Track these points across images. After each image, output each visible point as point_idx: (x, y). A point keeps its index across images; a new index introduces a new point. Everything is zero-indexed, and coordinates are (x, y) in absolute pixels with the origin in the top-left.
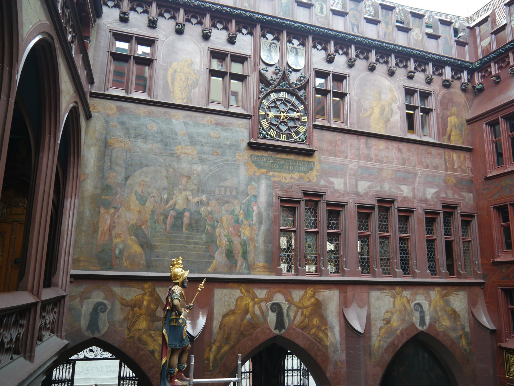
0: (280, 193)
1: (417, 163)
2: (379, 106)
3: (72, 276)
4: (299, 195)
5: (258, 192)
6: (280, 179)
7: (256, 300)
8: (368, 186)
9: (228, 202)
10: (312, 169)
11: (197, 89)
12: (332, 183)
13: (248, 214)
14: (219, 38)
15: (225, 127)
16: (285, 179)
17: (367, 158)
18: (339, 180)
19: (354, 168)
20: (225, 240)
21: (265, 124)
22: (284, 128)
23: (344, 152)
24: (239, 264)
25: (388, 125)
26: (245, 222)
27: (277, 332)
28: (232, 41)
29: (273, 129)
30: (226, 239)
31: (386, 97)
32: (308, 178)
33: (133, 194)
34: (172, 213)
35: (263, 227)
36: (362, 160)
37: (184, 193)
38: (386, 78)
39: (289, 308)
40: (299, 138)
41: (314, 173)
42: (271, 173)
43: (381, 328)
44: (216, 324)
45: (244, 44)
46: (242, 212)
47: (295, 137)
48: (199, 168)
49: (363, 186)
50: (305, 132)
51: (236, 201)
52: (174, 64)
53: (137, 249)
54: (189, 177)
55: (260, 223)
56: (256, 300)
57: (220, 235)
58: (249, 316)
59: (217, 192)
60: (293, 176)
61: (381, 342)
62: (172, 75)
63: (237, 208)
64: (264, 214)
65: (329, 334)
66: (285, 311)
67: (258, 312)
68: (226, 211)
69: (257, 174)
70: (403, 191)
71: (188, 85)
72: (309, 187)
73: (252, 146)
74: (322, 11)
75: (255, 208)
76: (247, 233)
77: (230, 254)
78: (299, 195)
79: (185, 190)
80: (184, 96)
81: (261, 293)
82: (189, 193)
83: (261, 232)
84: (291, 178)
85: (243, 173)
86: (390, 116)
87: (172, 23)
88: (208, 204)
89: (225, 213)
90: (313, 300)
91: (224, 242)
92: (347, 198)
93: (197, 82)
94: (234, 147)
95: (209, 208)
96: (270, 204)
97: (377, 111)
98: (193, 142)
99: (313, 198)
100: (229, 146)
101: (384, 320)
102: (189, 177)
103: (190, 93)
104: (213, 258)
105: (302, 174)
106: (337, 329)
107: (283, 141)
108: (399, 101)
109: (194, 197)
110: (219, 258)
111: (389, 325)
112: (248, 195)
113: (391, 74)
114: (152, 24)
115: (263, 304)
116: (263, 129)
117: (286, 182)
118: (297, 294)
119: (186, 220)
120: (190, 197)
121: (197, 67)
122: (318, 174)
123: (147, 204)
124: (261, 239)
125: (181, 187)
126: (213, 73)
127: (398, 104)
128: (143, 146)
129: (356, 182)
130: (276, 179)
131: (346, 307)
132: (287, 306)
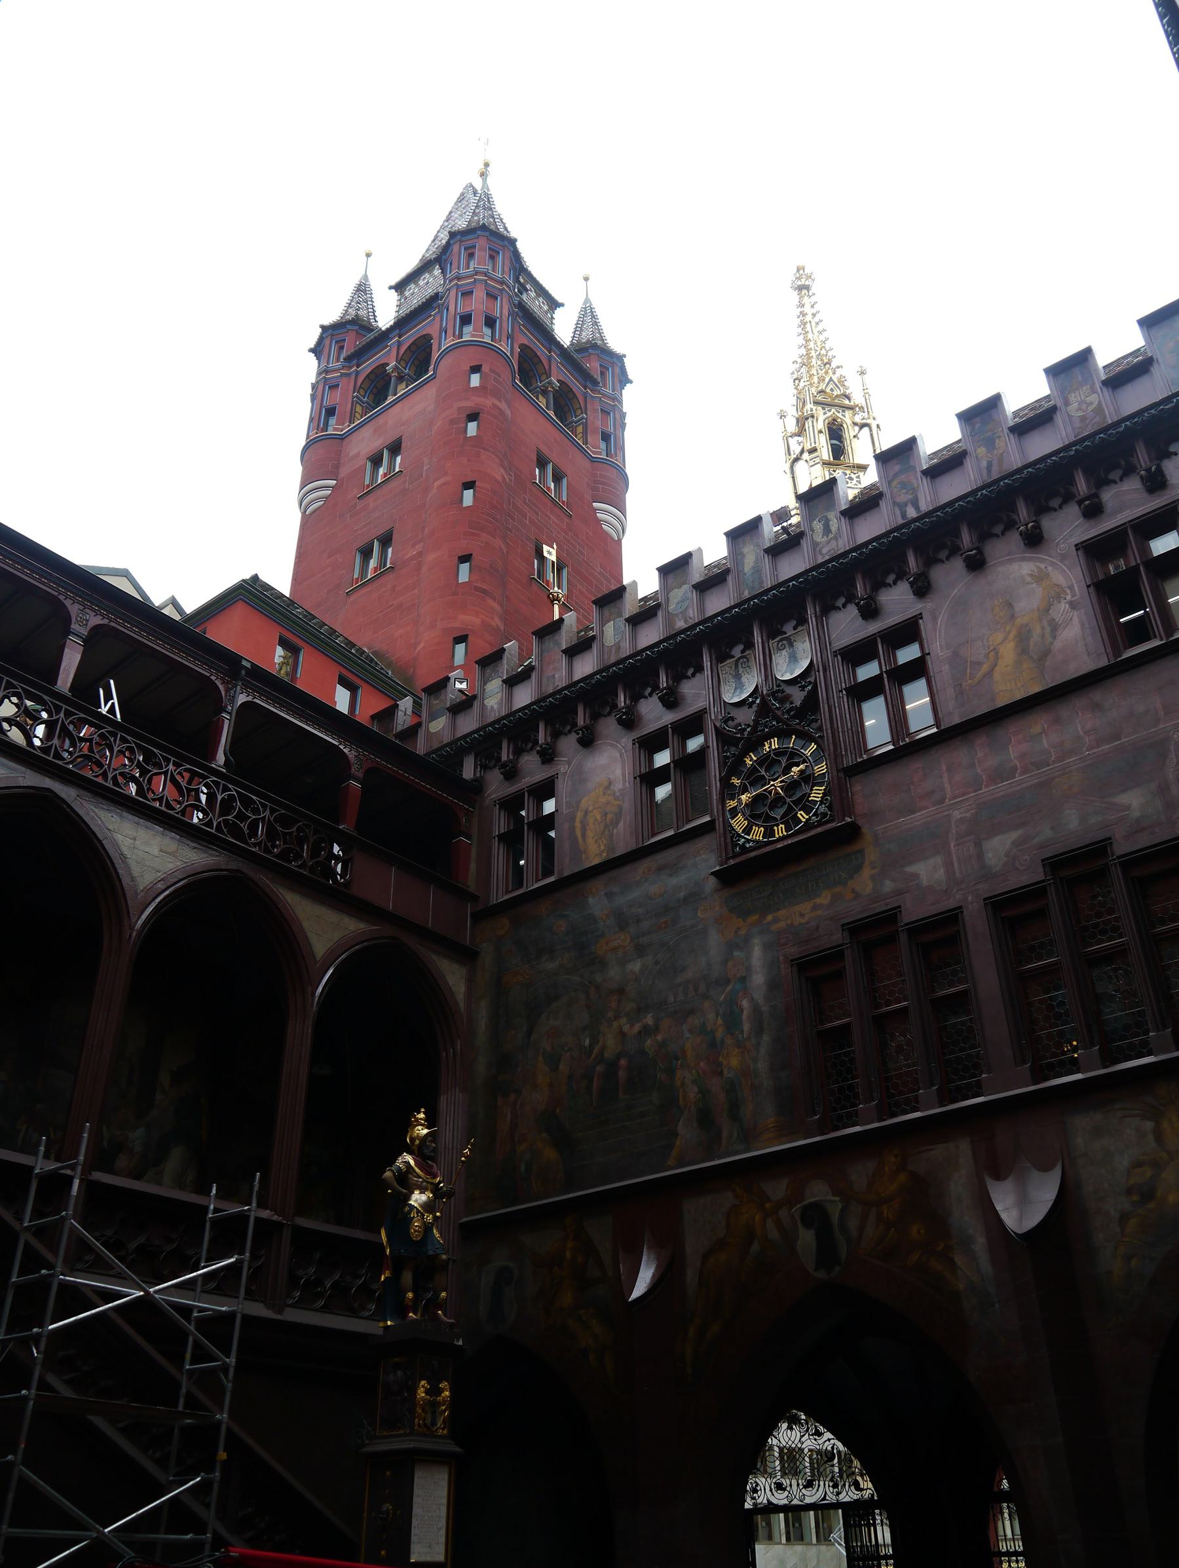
0: (793, 951)
1: (1161, 713)
2: (1012, 636)
3: (463, 1226)
4: (838, 937)
5: (749, 969)
6: (789, 922)
7: (767, 1205)
8: (1013, 843)
9: (692, 1012)
10: (859, 868)
11: (621, 824)
12: (916, 876)
13: (732, 1021)
14: (654, 714)
15: (673, 868)
16: (802, 915)
17: (998, 775)
18: (932, 861)
19: (967, 815)
20: (693, 1092)
21: (739, 823)
22: (778, 813)
23: (933, 792)
24: (725, 1134)
25: (1048, 663)
26: (729, 1041)
27: (821, 1275)
28: (671, 701)
29: (757, 825)
30: (696, 1089)
31: (1028, 603)
32: (853, 891)
33: (540, 1058)
34: (599, 1069)
35: (766, 1038)
36: (986, 786)
37: (615, 1024)
38: (1030, 559)
39: (843, 1211)
40: (815, 814)
41: (866, 872)
42: (770, 918)
43: (1124, 1218)
44: (691, 1276)
45: (695, 693)
46: (720, 1021)
47: (802, 816)
48: (636, 966)
49: (998, 849)
50: (824, 794)
51: (707, 1004)
52: (585, 803)
53: (551, 1154)
54: (621, 991)
55: (759, 1030)
56: (767, 1205)
57: (683, 1084)
58: (756, 1247)
59: (672, 999)
60: (818, 901)
61: (1133, 1262)
62: (581, 822)
63: (711, 1016)
64: (764, 1009)
65: (959, 1259)
66: (835, 1219)
67: (774, 1234)
68: (690, 1031)
69: (742, 932)
70: (1128, 808)
71: (606, 826)
72: (855, 910)
73: (726, 877)
74: (827, 530)
75: (745, 1003)
76: (734, 1062)
77: (705, 1118)
78: (838, 937)
79: (617, 1017)
80: (602, 848)
81: (778, 1189)
82: (624, 1020)
83: (763, 1051)
84: (815, 908)
85: (715, 940)
86: (1049, 639)
87: (574, 737)
88: (656, 1029)
89: (688, 1035)
90: (902, 1178)
91: (692, 1095)
92: (958, 896)
93: (619, 814)
94: (693, 898)
95: (659, 1038)
96: (773, 985)
97: (1008, 652)
98: (622, 921)
99: (875, 931)
100: (685, 899)
101: (1129, 1192)
102: (621, 991)
103: (611, 836)
104: (676, 1134)
105: (837, 889)
106: (980, 1243)
107: (781, 839)
108: (1071, 588)
109: (632, 1026)
110: (686, 1132)
111: (1151, 1206)
112: (728, 981)
113: (1034, 540)
114: (548, 756)
115: (783, 1213)
116: (739, 835)
117: (803, 921)
118: (860, 1173)
119: (622, 1074)
120: (626, 1028)
121: (618, 786)
122: (874, 871)
123: (561, 1067)
124: (762, 1066)
125: (610, 1014)
126: (654, 778)
127: (1069, 597)
128: (550, 966)
129: (978, 844)
130: (781, 925)
131: (999, 1177)
132: (840, 1205)
